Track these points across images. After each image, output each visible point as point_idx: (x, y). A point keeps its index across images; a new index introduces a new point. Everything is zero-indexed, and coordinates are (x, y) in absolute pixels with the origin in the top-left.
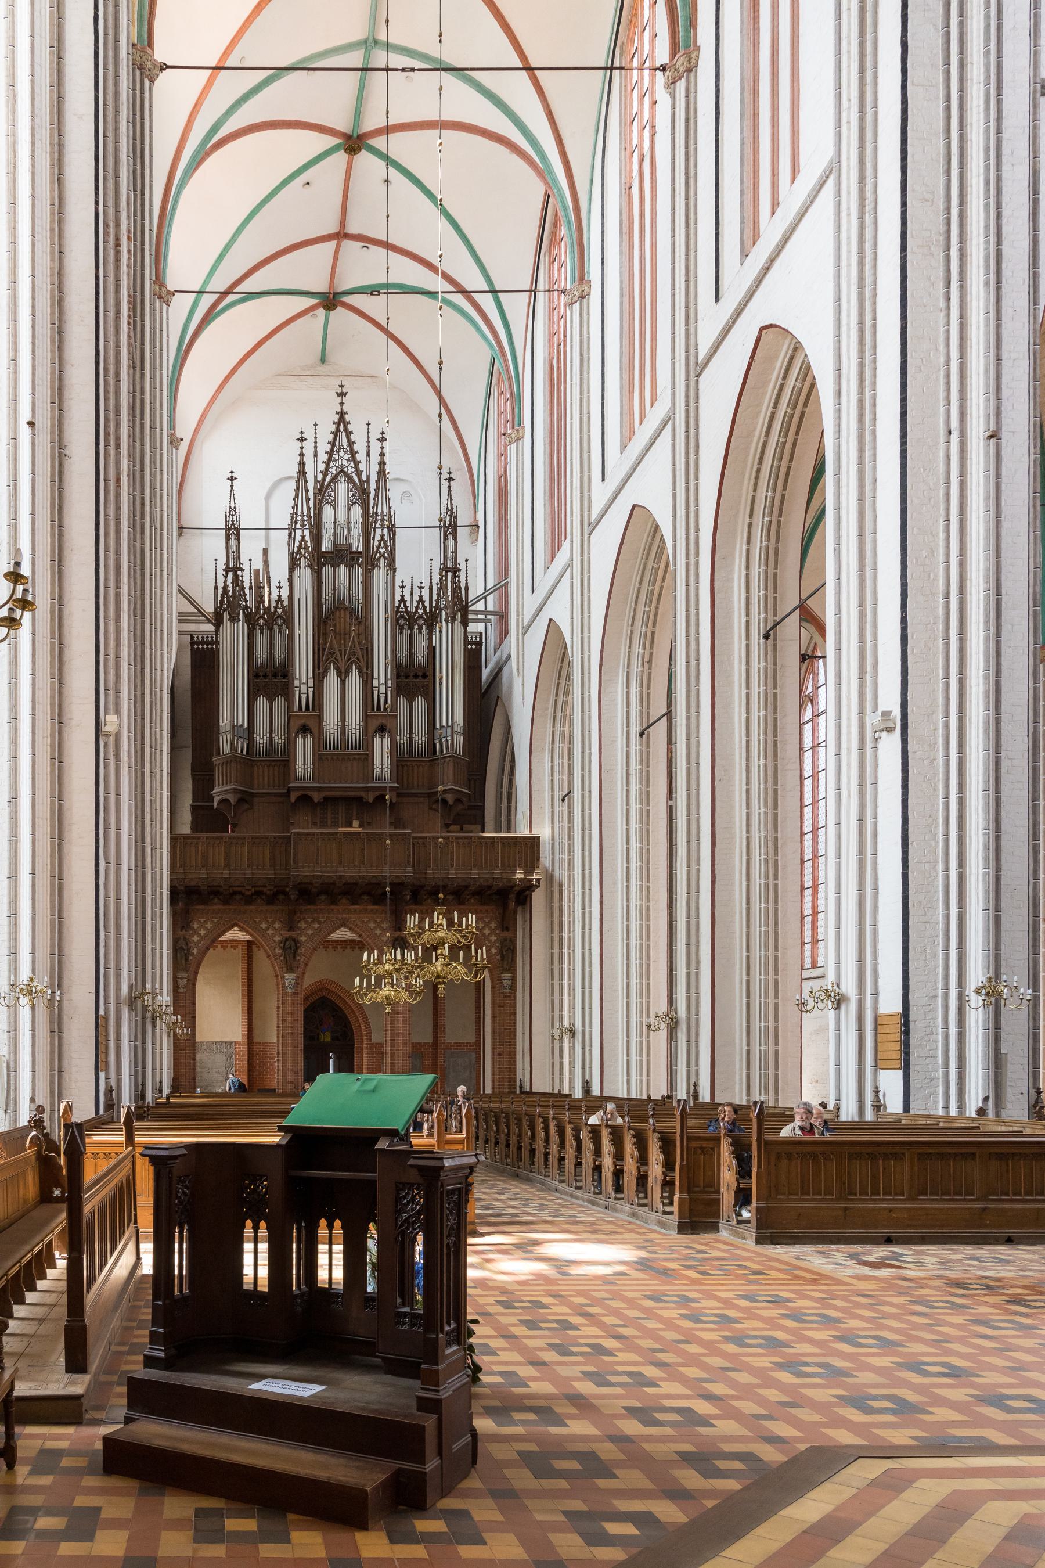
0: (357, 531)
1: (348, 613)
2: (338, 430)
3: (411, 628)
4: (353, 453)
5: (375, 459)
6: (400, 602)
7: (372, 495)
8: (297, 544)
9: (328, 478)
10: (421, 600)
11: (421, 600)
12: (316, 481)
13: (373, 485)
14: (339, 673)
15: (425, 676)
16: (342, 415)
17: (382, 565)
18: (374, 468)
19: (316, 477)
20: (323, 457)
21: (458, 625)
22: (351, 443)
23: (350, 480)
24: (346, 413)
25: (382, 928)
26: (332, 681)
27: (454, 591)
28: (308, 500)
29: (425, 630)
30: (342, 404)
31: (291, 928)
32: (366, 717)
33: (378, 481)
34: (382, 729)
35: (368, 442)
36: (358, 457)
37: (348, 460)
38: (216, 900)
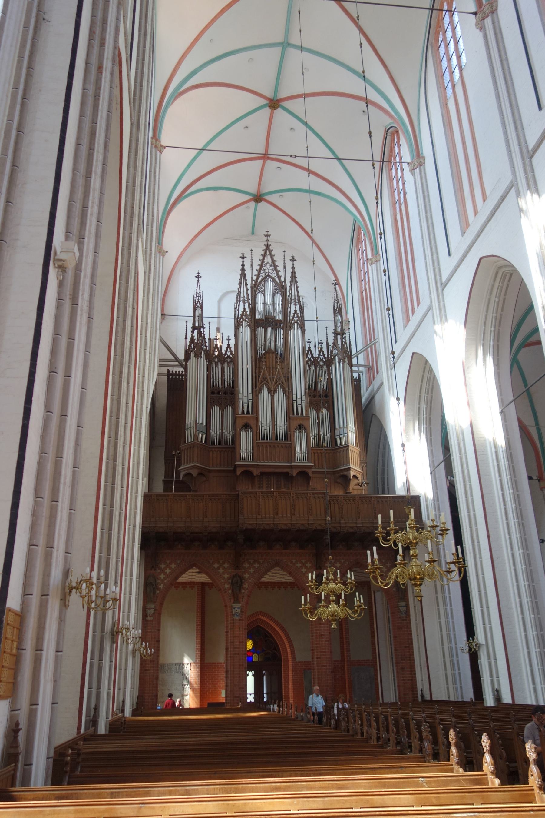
0: (279, 308)
1: (274, 356)
2: (265, 254)
3: (316, 367)
4: (275, 267)
6: (308, 351)
7: (288, 289)
8: (240, 313)
9: (260, 279)
11: (321, 350)
12: (252, 280)
13: (288, 284)
14: (270, 391)
16: (268, 246)
19: (252, 278)
20: (256, 267)
22: (274, 261)
23: (273, 280)
24: (270, 245)
25: (306, 568)
26: (265, 396)
27: (343, 346)
28: (247, 290)
29: (325, 368)
31: (237, 567)
32: (289, 419)
33: (291, 282)
34: (301, 427)
35: (284, 261)
36: (278, 269)
37: (272, 270)
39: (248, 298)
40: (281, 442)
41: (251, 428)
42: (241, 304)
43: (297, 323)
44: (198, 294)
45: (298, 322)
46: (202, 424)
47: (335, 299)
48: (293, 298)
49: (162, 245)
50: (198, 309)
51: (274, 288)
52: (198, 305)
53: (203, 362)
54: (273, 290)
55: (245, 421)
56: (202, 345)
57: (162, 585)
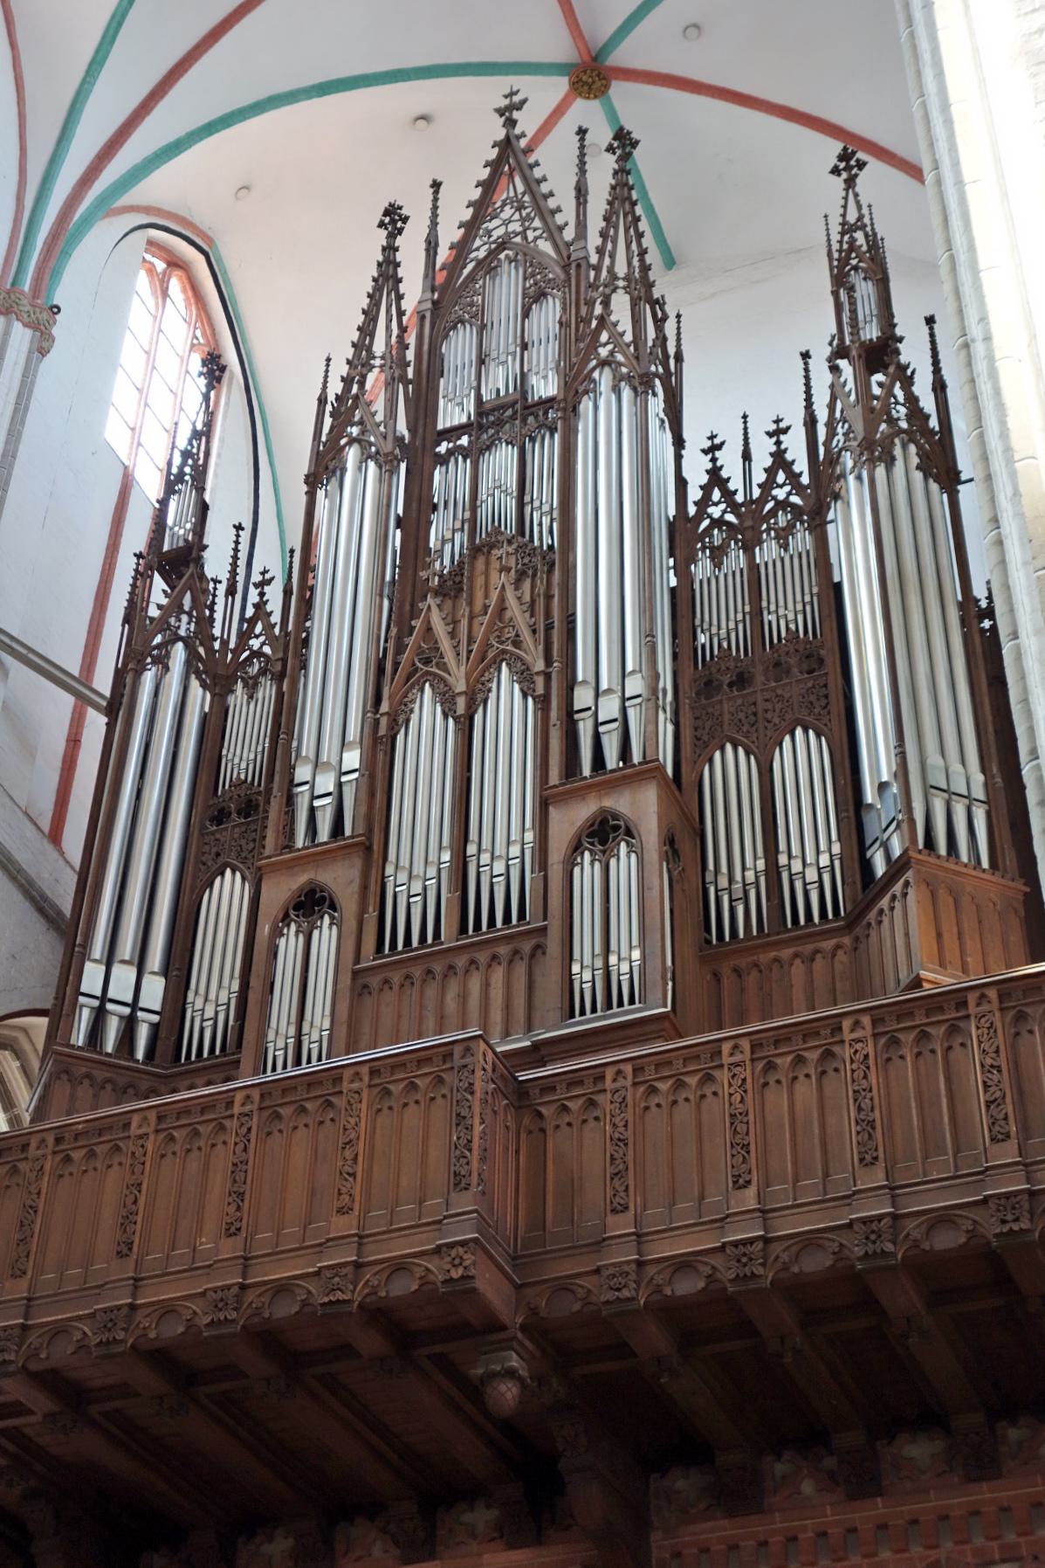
10: (780, 459)
11: (780, 459)
29: (802, 540)
54: (524, 289)
55: (301, 879)
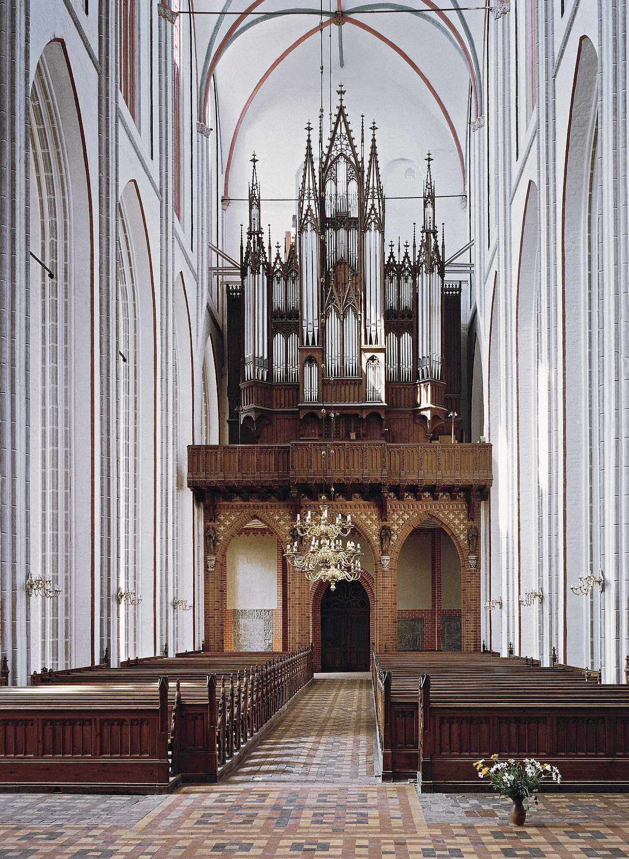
2: (338, 120)
4: (351, 140)
5: (368, 143)
7: (366, 173)
10: (406, 256)
11: (406, 256)
12: (321, 162)
13: (366, 165)
15: (410, 316)
16: (341, 109)
17: (373, 228)
18: (368, 151)
20: (326, 143)
21: (436, 276)
22: (349, 132)
23: (348, 160)
25: (371, 520)
26: (333, 322)
30: (341, 100)
33: (370, 162)
36: (355, 143)
37: (347, 145)
38: (238, 498)
39: (315, 188)
40: (351, 377)
41: (316, 362)
42: (306, 203)
43: (375, 222)
44: (254, 187)
45: (376, 221)
46: (263, 357)
47: (427, 182)
48: (371, 186)
49: (205, 122)
50: (255, 207)
51: (349, 172)
52: (255, 201)
53: (262, 279)
56: (259, 257)
57: (222, 537)
